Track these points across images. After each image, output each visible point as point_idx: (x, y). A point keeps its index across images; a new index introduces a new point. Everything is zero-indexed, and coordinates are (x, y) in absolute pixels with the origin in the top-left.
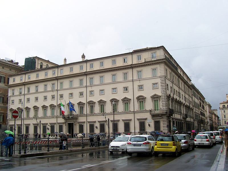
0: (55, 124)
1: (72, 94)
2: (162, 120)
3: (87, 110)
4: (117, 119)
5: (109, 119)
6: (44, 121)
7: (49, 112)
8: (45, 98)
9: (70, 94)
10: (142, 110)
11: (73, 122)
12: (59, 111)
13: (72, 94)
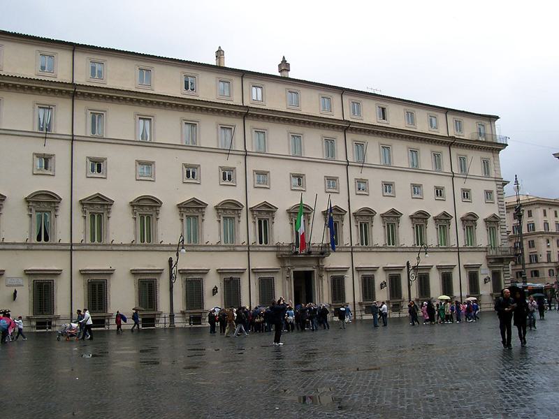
0: (241, 272)
1: (299, 177)
2: (502, 269)
3: (349, 233)
4: (426, 263)
5: (408, 263)
6: (188, 261)
7: (211, 229)
8: (191, 173)
9: (295, 176)
10: (472, 248)
11: (311, 269)
12: (254, 229)
13: (299, 177)
